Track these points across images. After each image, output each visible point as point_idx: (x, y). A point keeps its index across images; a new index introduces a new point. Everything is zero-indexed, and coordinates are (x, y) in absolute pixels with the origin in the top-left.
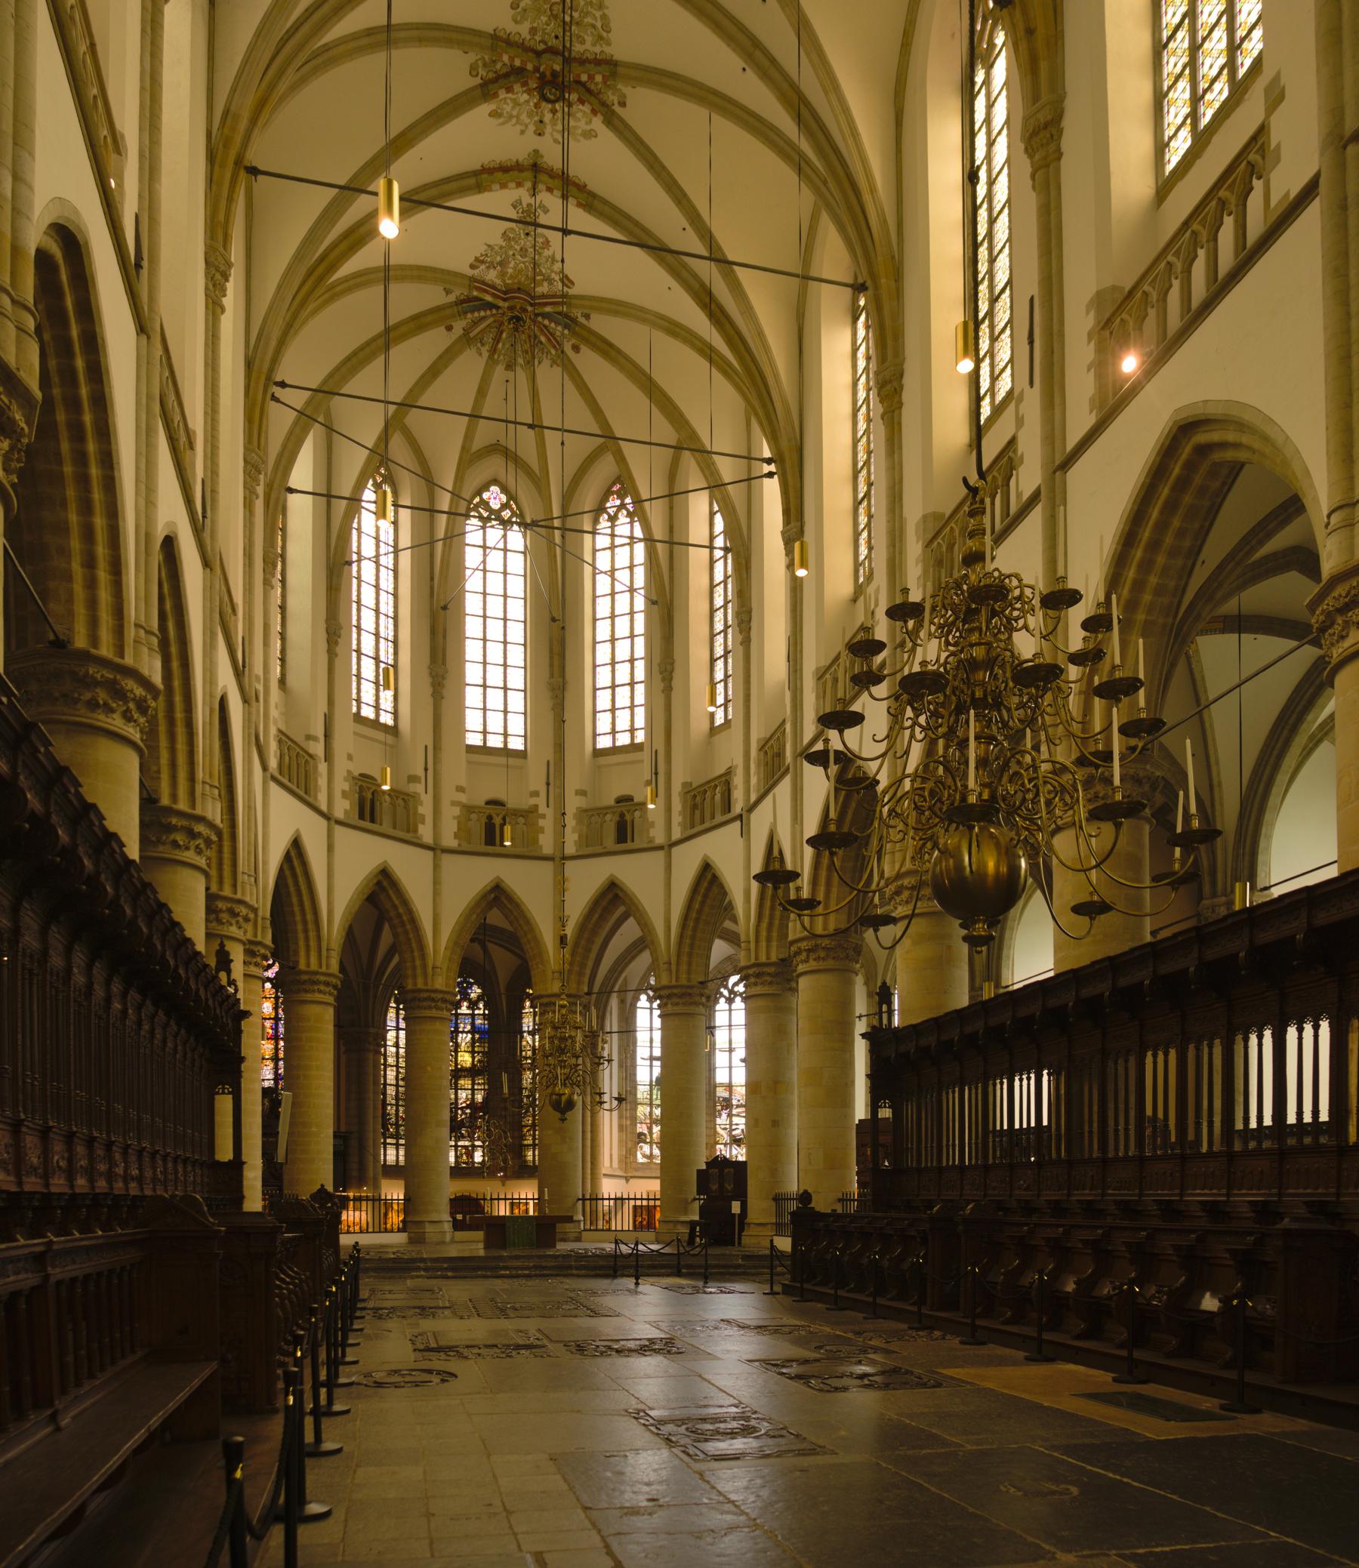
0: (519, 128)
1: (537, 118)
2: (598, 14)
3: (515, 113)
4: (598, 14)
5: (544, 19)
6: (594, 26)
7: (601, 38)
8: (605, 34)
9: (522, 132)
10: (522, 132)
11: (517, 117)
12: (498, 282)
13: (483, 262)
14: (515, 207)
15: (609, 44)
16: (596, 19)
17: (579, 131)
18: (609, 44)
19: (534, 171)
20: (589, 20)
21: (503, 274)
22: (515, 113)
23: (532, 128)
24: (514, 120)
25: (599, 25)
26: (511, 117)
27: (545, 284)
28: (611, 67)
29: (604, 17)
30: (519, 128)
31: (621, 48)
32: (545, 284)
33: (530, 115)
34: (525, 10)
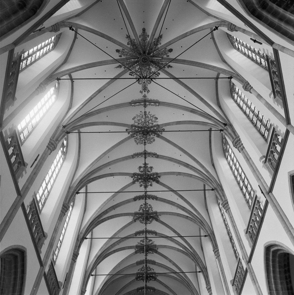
0: (150, 113)
1: (146, 116)
2: (138, 142)
3: (152, 118)
4: (138, 142)
5: (148, 137)
6: (138, 139)
7: (136, 139)
8: (135, 139)
9: (149, 112)
10: (149, 112)
11: (151, 117)
12: (151, 67)
13: (156, 75)
14: (149, 90)
15: (134, 139)
16: (138, 141)
17: (136, 117)
18: (134, 139)
19: (145, 102)
20: (139, 140)
21: (149, 69)
22: (152, 118)
23: (147, 113)
24: (152, 116)
25: (137, 140)
26: (152, 117)
27: (137, 69)
28: (132, 136)
29: (136, 142)
30: (150, 113)
31: (133, 140)
32: (137, 69)
33: (148, 117)
34: (152, 139)
